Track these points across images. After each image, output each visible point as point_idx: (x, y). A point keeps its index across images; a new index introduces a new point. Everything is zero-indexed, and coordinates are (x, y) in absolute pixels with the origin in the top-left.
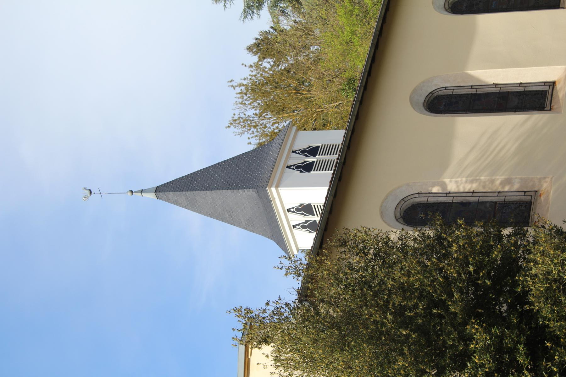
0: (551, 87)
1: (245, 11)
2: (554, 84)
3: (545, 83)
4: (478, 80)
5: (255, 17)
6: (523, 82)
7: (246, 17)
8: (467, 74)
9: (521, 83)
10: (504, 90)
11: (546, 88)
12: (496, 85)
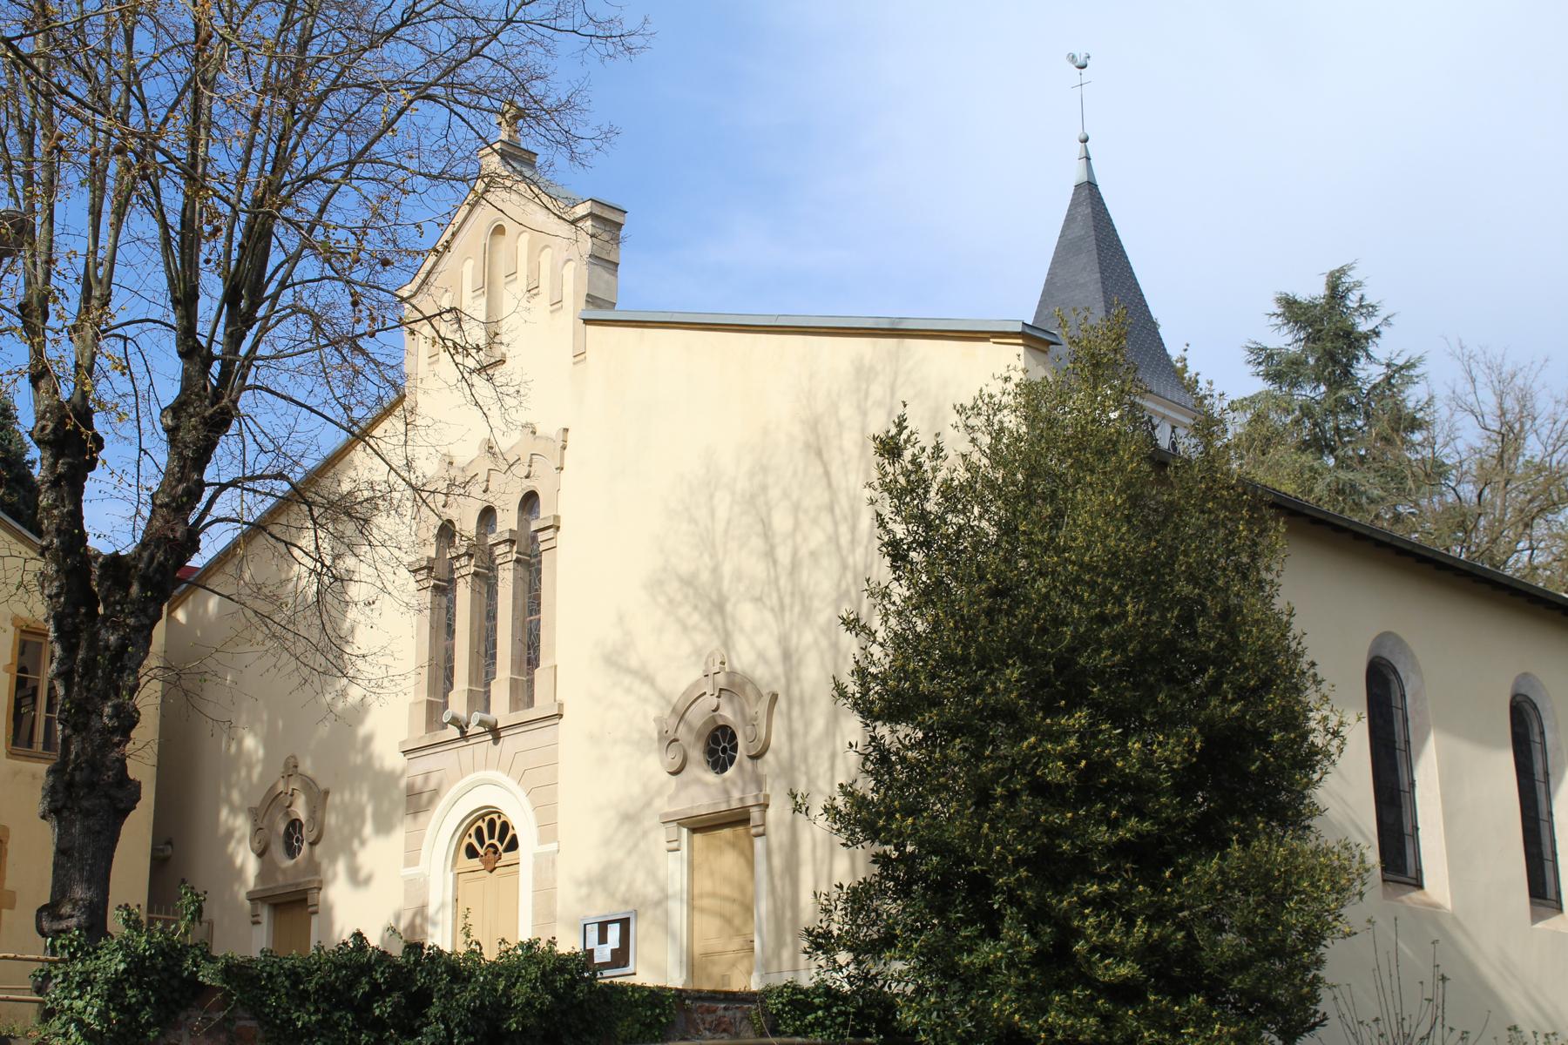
0: (1414, 882)
1: (1265, 349)
2: (1419, 885)
3: (1419, 871)
5: (1251, 369)
6: (1420, 833)
7: (1252, 351)
9: (1417, 829)
11: (1411, 872)
12: (1412, 784)
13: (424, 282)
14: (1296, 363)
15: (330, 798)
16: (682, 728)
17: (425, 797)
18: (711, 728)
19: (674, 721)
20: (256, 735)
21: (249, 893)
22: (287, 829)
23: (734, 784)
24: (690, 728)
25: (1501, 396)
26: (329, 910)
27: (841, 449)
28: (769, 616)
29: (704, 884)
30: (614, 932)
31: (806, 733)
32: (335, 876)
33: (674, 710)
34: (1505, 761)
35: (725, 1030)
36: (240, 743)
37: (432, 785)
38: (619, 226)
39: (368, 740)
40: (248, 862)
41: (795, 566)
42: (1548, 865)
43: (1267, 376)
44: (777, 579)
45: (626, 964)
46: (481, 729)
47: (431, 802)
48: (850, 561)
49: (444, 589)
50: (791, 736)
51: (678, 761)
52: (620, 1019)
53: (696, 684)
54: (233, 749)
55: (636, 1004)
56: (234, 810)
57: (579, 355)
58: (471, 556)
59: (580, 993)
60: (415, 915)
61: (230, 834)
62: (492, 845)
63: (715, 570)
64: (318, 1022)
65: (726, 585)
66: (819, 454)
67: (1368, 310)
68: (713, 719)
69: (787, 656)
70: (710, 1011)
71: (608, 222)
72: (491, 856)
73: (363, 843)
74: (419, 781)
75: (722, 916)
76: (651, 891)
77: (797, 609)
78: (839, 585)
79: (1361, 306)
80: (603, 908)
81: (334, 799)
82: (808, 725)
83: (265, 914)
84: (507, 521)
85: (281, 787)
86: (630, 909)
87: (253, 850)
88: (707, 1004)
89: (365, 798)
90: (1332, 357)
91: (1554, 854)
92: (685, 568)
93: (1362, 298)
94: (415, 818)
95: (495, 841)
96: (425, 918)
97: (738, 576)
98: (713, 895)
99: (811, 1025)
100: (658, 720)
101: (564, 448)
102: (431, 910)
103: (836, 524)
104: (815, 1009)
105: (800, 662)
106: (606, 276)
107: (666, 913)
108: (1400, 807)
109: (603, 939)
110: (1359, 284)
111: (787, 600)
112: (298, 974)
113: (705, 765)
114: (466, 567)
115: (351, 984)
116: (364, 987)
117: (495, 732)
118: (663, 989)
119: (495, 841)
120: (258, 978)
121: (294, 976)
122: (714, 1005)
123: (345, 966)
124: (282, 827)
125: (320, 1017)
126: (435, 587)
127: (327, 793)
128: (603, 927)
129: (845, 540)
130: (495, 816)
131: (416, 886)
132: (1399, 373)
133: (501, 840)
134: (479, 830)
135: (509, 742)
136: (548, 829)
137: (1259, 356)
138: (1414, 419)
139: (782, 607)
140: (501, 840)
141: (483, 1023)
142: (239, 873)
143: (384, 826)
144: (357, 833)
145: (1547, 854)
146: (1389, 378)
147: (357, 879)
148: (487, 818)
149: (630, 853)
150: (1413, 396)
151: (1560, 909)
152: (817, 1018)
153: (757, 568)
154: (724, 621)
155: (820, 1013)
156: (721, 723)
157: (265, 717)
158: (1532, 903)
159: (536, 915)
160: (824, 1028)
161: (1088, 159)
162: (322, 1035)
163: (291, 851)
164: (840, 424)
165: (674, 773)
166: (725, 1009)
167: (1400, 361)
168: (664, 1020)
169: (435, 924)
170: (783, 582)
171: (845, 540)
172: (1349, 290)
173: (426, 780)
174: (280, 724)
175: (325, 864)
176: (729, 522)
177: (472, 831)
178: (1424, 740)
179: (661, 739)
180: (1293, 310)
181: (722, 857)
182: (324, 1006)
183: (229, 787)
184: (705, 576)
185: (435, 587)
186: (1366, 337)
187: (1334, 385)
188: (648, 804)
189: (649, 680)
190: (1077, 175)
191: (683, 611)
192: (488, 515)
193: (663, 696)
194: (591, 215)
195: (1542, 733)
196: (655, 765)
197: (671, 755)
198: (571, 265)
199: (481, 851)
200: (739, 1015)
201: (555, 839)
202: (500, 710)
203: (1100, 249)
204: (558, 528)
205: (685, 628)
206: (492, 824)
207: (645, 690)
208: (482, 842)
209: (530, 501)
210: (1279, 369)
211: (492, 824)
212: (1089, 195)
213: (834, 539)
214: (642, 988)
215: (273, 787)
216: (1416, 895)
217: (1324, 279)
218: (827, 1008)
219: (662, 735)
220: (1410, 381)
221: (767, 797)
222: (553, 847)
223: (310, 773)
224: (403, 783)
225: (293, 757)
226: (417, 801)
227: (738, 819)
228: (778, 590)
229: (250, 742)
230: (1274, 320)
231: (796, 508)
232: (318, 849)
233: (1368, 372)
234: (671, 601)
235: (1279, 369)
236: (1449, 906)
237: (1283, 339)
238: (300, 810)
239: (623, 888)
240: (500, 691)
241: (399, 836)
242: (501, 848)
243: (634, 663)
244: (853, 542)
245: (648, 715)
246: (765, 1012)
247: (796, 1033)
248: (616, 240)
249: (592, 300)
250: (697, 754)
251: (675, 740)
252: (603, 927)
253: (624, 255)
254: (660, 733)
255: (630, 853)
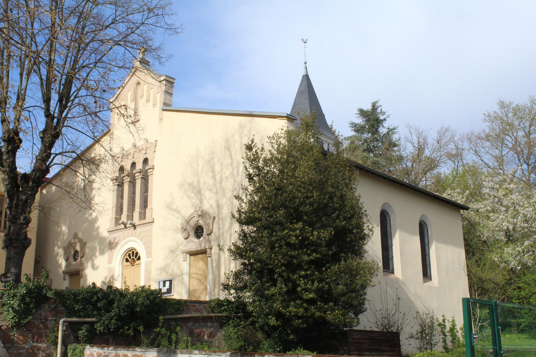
1: (354, 123)
3: (393, 269)
4: (394, 236)
5: (351, 129)
7: (351, 124)
8: (397, 231)
10: (390, 249)
11: (391, 269)
12: (392, 245)
13: (117, 97)
14: (363, 127)
15: (87, 245)
16: (188, 226)
17: (114, 245)
18: (196, 226)
19: (185, 224)
20: (66, 226)
21: (63, 271)
22: (74, 253)
23: (203, 242)
24: (190, 226)
25: (419, 138)
26: (86, 276)
27: (235, 148)
28: (213, 195)
29: (194, 270)
30: (167, 284)
31: (223, 228)
32: (88, 267)
33: (186, 221)
34: (417, 239)
35: (198, 312)
36: (61, 228)
37: (116, 241)
38: (173, 83)
39: (98, 228)
40: (63, 263)
41: (221, 181)
42: (428, 268)
43: (355, 131)
44: (216, 184)
45: (171, 293)
46: (131, 226)
47: (116, 246)
48: (237, 180)
49: (120, 185)
50: (219, 229)
51: (187, 235)
52: (168, 308)
53: (192, 214)
54: (59, 230)
55: (173, 304)
56: (59, 247)
57: (161, 120)
58: (128, 176)
59: (157, 300)
60: (111, 278)
61: (58, 254)
62: (133, 259)
63: (199, 182)
64: (81, 308)
65: (201, 186)
66: (229, 149)
67: (383, 113)
68: (197, 223)
69: (218, 206)
70: (194, 306)
71: (170, 82)
72: (133, 261)
73: (96, 257)
74: (112, 240)
75: (198, 279)
76: (178, 272)
77: (221, 193)
78: (233, 186)
79: (381, 112)
80: (164, 277)
81: (88, 245)
82: (224, 226)
83: (67, 277)
84: (139, 166)
85: (72, 241)
86: (172, 277)
87: (64, 259)
88: (193, 304)
89: (97, 244)
90: (373, 126)
91: (430, 264)
92: (190, 181)
93: (381, 110)
94: (111, 250)
95: (134, 257)
96: (113, 279)
97: (205, 183)
98: (196, 273)
99: (223, 310)
100: (181, 224)
101: (156, 146)
102: (115, 277)
103: (233, 169)
104: (224, 306)
105: (222, 208)
106: (169, 97)
107: (183, 278)
108: (388, 251)
109: (164, 286)
110: (381, 106)
111: (219, 191)
112: (76, 294)
113: (194, 237)
114: (127, 180)
115: (91, 298)
116: (95, 298)
117: (134, 226)
118: (181, 300)
119: (134, 257)
120: (65, 295)
121: (75, 295)
122: (195, 304)
123: (90, 292)
124: (73, 252)
125: (82, 307)
126: (118, 185)
127: (86, 243)
128: (164, 282)
129: (235, 173)
130: (134, 250)
131: (111, 270)
132: (391, 131)
133: (136, 257)
134: (129, 255)
135: (138, 229)
136: (149, 254)
137: (352, 125)
138: (395, 144)
139: (217, 192)
140: (136, 257)
141: (129, 309)
142: (60, 266)
143: (102, 253)
144: (94, 254)
145: (428, 264)
146: (388, 132)
147: (94, 267)
148: (132, 251)
149: (172, 261)
150: (395, 137)
151: (431, 279)
152: (225, 308)
153: (210, 181)
154: (201, 196)
155: (226, 307)
156: (199, 225)
157: (68, 221)
158: (423, 278)
159: (145, 278)
160: (227, 311)
161: (306, 68)
162: (83, 312)
163: (75, 259)
164: (235, 141)
165: (186, 239)
166: (199, 306)
167: (391, 128)
168: (181, 309)
169: (116, 280)
170: (218, 185)
171: (235, 173)
172: (378, 107)
173: (115, 240)
174: (73, 223)
175: (85, 263)
176: (203, 168)
177: (127, 254)
178: (395, 233)
179: (182, 229)
180: (362, 113)
181: (199, 263)
182: (83, 303)
183: (58, 241)
184: (195, 183)
185: (118, 185)
186: (382, 121)
187: (373, 134)
188: (178, 248)
189: (178, 212)
190: (303, 73)
191: (189, 193)
192: (134, 165)
193: (183, 217)
194: (165, 80)
195: (427, 231)
196: (180, 237)
197: (185, 234)
198: (159, 94)
199: (130, 260)
200: (202, 307)
201: (151, 257)
202: (136, 220)
203: (309, 94)
204: (154, 169)
205: (190, 198)
206: (133, 253)
207: (178, 215)
208: (130, 257)
209: (146, 161)
210: (358, 129)
211: (133, 253)
212: (306, 78)
213: (232, 173)
214: (175, 299)
215: (70, 241)
216: (392, 275)
217: (371, 104)
218: (228, 306)
219: (182, 228)
220: (394, 133)
221: (212, 246)
222: (150, 259)
223: (81, 237)
224: (108, 240)
225: (76, 232)
226: (112, 246)
227: (203, 252)
228: (216, 187)
229: (64, 228)
230: (357, 115)
231: (222, 164)
232: (83, 259)
233: (383, 130)
234: (186, 190)
235: (358, 129)
236: (401, 278)
237: (360, 121)
238: (78, 248)
239: (170, 271)
240: (136, 215)
241: (106, 256)
242: (136, 259)
243: (175, 207)
244: (238, 174)
245: (178, 222)
246: (210, 306)
247: (219, 313)
248: (172, 87)
249: (165, 104)
250: (192, 233)
251: (186, 229)
252: (164, 282)
253: (174, 91)
254: (182, 227)
255: (172, 261)
